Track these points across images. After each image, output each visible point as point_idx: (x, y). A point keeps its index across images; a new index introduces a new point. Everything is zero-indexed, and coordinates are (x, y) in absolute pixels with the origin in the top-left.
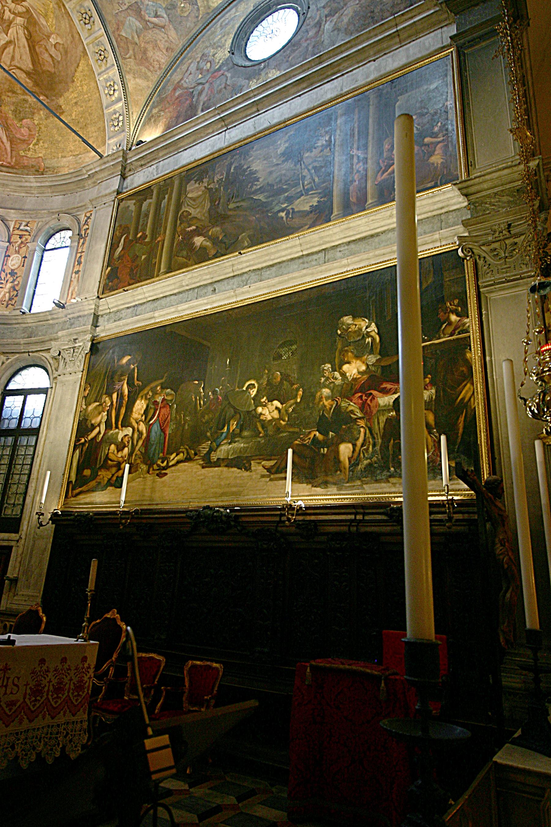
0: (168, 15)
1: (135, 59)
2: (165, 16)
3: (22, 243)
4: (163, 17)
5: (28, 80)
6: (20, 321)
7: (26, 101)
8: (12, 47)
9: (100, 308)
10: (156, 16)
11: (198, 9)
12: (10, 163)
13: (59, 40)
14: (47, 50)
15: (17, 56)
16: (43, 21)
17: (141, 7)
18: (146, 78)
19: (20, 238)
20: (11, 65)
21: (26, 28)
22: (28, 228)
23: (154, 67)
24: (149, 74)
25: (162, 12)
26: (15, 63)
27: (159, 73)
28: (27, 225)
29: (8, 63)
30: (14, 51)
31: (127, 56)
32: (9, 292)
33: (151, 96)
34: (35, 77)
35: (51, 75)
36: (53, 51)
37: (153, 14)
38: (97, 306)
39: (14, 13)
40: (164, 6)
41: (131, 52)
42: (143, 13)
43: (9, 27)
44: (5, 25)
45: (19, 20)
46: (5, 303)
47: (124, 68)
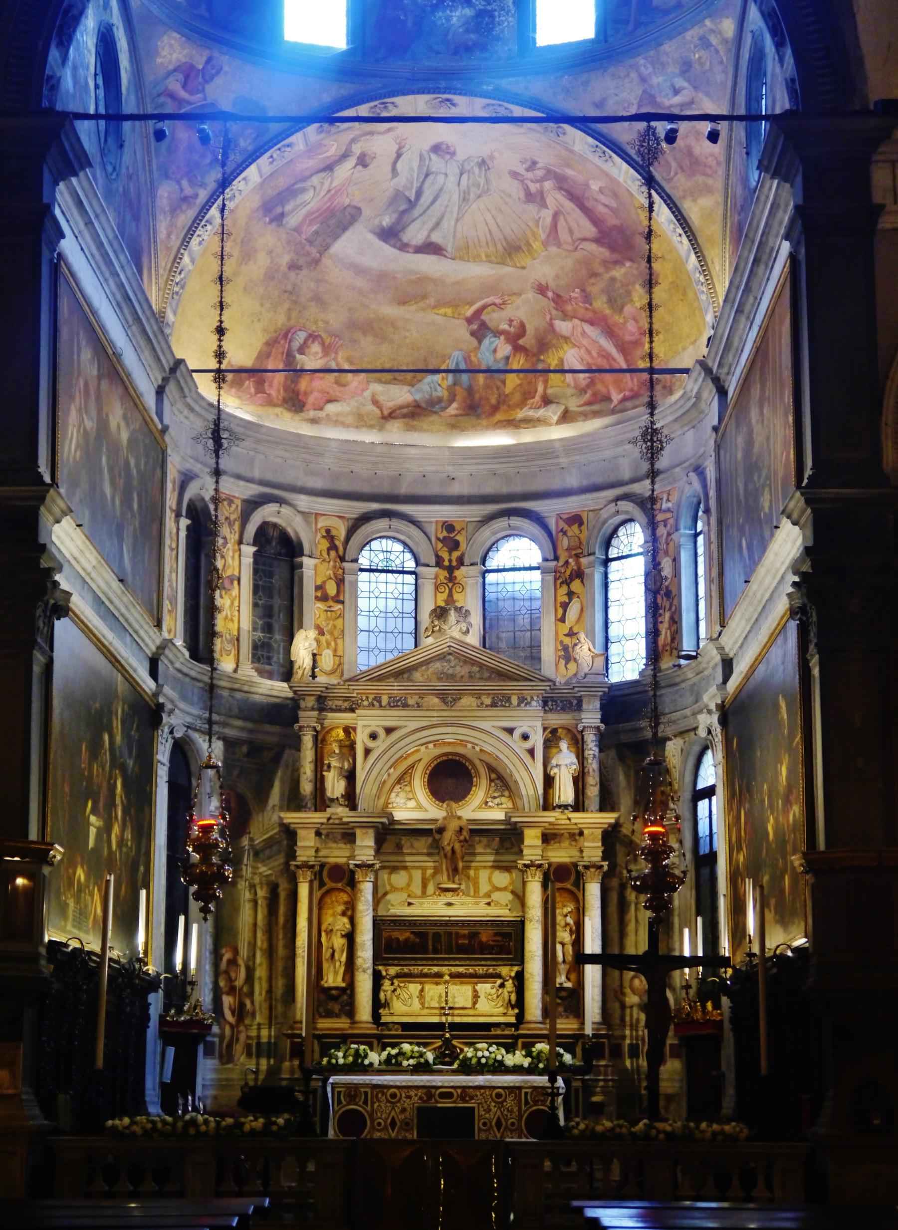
0: (689, 81)
1: (683, 171)
2: (686, 84)
3: (669, 534)
4: (684, 89)
5: (602, 250)
6: (683, 677)
7: (613, 279)
8: (562, 218)
9: (727, 650)
10: (676, 92)
11: (717, 51)
12: (632, 390)
13: (600, 184)
14: (596, 200)
15: (573, 225)
16: (569, 172)
17: (653, 92)
18: (709, 190)
19: (665, 526)
20: (574, 242)
21: (560, 189)
22: (670, 505)
23: (710, 167)
24: (710, 181)
25: (680, 82)
26: (577, 235)
27: (721, 172)
28: (668, 500)
29: (569, 240)
30: (567, 222)
31: (672, 174)
32: (669, 628)
33: (725, 215)
34: (606, 241)
35: (620, 229)
36: (603, 199)
37: (670, 92)
38: (721, 649)
39: (537, 181)
40: (677, 71)
41: (674, 165)
42: (659, 100)
43: (543, 199)
44: (538, 200)
45: (548, 185)
46: (668, 648)
47: (675, 194)
